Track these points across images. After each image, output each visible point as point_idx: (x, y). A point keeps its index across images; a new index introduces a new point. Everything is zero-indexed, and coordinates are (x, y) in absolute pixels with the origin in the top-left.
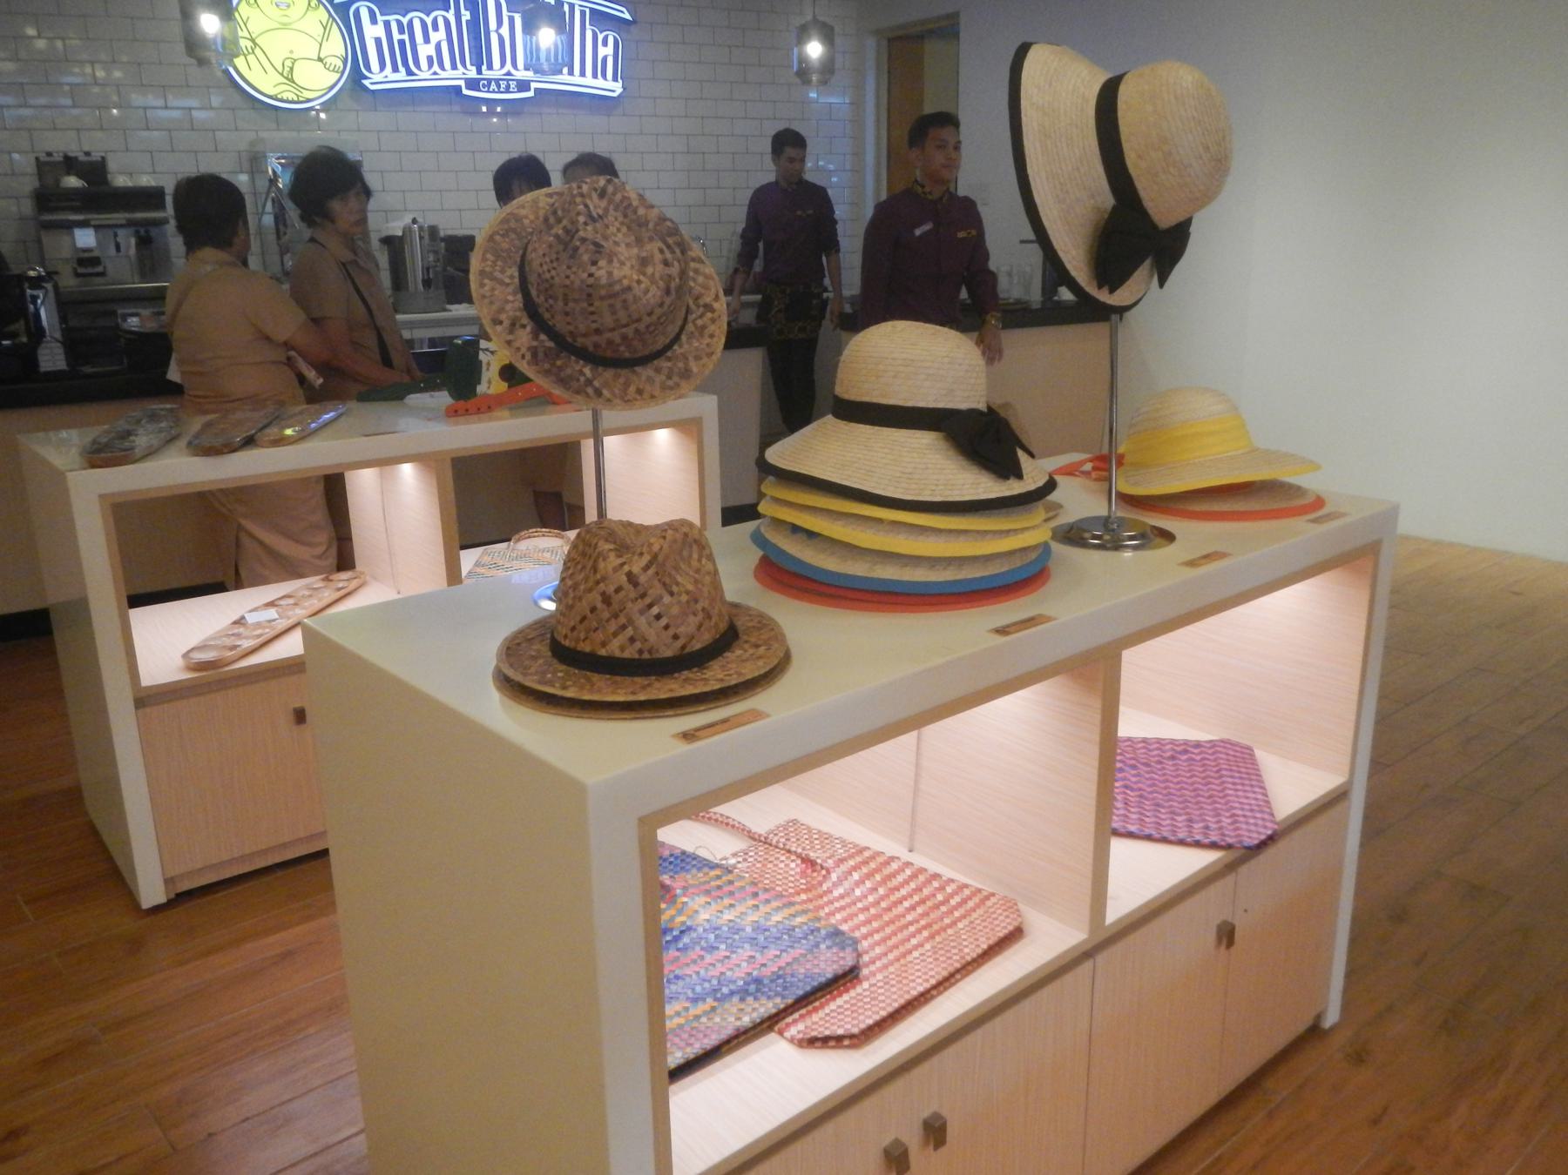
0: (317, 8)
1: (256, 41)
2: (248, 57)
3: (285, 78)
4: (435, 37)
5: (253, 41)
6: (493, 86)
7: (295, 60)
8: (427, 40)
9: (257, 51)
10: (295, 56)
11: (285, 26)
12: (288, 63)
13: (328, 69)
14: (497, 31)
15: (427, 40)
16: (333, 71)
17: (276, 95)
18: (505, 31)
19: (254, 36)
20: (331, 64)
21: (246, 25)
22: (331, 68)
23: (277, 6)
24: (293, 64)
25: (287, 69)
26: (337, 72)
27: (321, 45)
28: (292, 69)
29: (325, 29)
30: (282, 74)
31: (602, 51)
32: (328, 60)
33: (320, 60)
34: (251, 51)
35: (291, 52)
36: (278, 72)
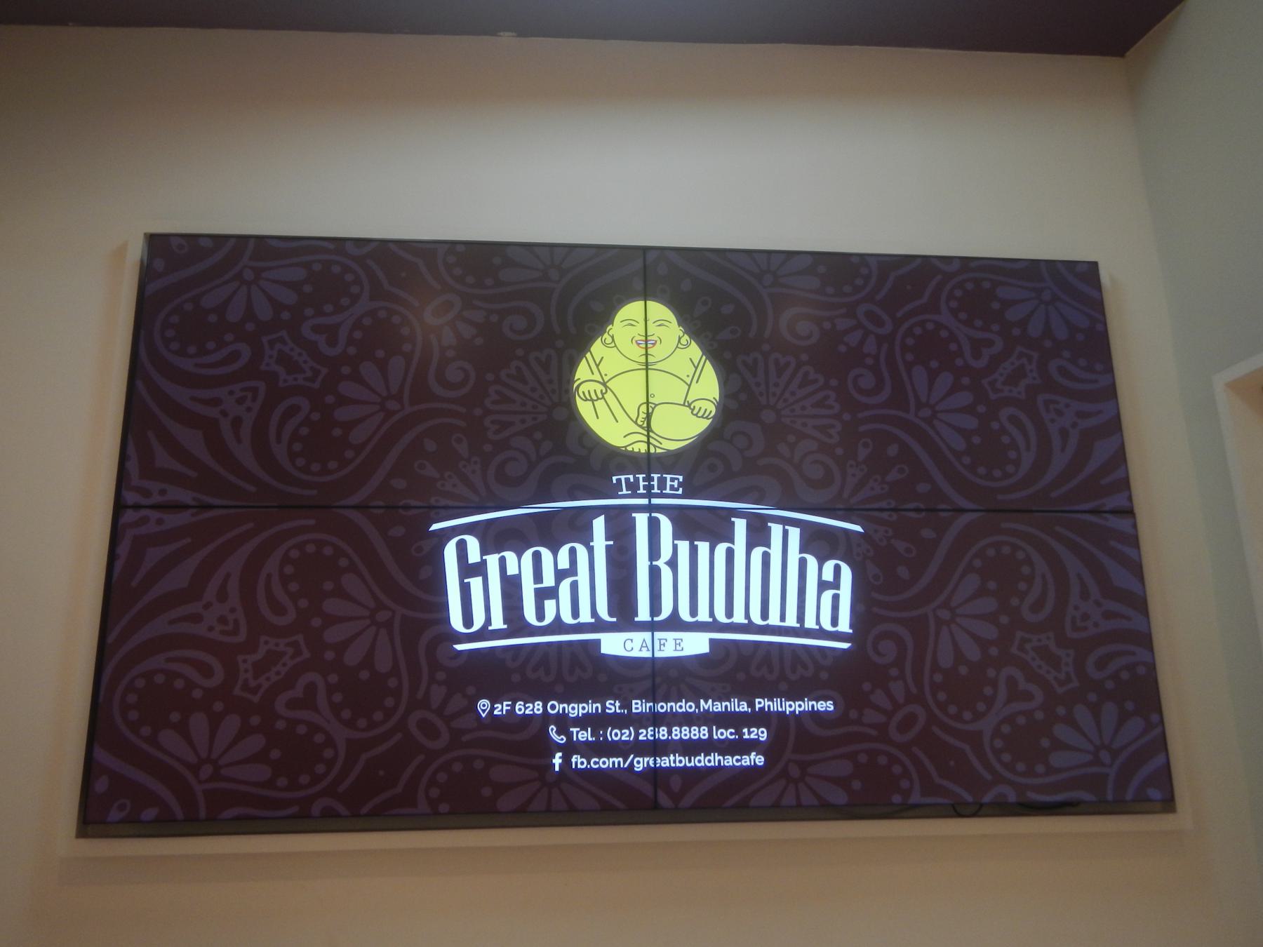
0: (688, 345)
1: (608, 384)
2: (595, 402)
3: (640, 426)
5: (604, 384)
7: (656, 405)
9: (609, 396)
13: (696, 415)
16: (702, 417)
17: (625, 447)
19: (606, 379)
20: (700, 408)
21: (597, 366)
22: (700, 414)
23: (638, 344)
25: (643, 416)
26: (707, 418)
27: (689, 386)
29: (696, 368)
30: (636, 422)
32: (697, 405)
34: (600, 396)
36: (632, 420)
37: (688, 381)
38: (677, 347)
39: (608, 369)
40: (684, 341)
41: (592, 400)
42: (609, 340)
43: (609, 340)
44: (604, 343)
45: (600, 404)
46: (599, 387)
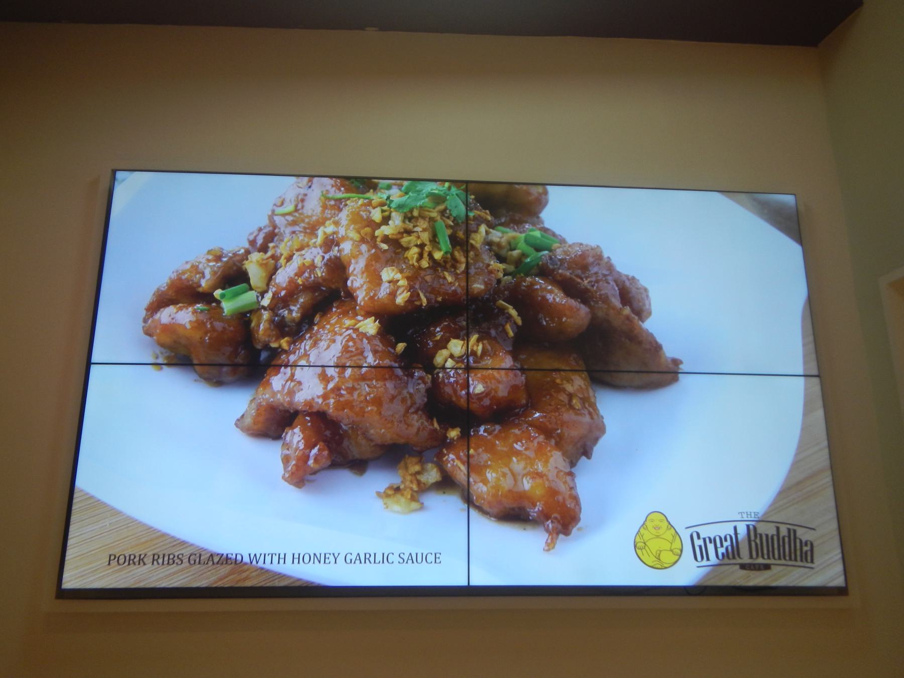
0: (670, 529)
1: (647, 544)
4: (725, 544)
5: (645, 543)
6: (752, 567)
8: (722, 546)
9: (647, 548)
10: (660, 549)
11: (658, 537)
12: (658, 552)
14: (755, 541)
15: (722, 546)
18: (758, 541)
21: (642, 537)
24: (660, 552)
25: (658, 555)
27: (671, 544)
28: (659, 555)
31: (805, 549)
33: (671, 550)
35: (660, 547)
37: (671, 542)
38: (667, 530)
39: (646, 537)
40: (669, 527)
41: (641, 549)
42: (645, 527)
43: (645, 527)
44: (644, 528)
45: (644, 550)
46: (643, 545)
